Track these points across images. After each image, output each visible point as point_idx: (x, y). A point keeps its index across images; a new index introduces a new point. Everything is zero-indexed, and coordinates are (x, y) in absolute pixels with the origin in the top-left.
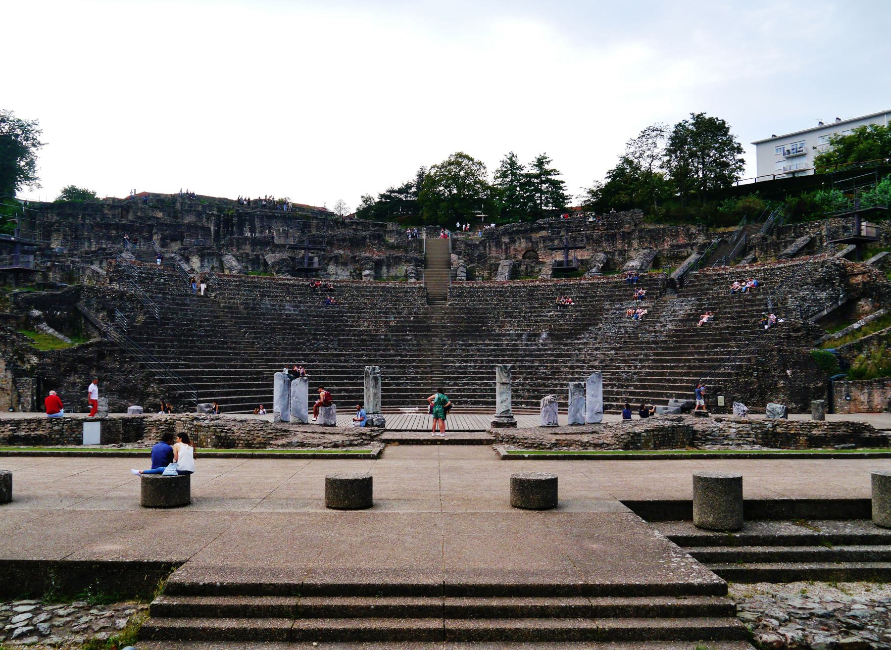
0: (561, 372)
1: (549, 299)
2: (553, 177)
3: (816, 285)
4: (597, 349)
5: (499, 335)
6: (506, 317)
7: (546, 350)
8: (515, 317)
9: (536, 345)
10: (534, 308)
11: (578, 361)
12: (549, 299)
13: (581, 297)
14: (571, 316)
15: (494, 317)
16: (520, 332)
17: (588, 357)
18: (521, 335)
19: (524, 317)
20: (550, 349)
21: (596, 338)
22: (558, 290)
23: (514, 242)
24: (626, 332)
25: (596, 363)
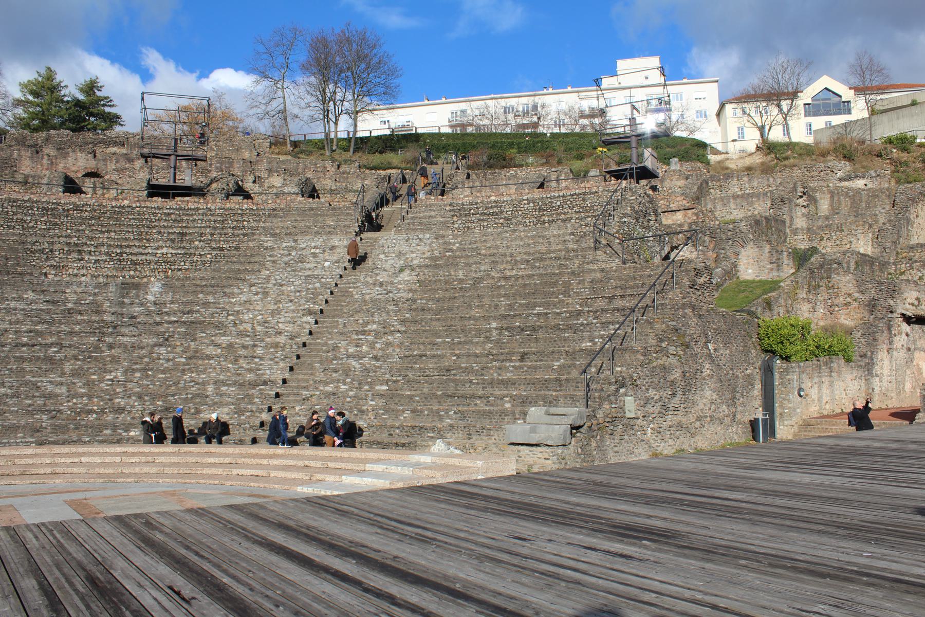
0: (209, 357)
1: (154, 227)
2: (107, 109)
3: (637, 219)
4: (273, 313)
5: (58, 283)
6: (69, 252)
7: (166, 313)
8: (90, 253)
9: (142, 304)
10: (126, 239)
11: (240, 334)
12: (154, 227)
13: (215, 228)
14: (205, 255)
15: (42, 251)
16: (101, 280)
17: (259, 328)
18: (106, 285)
19: (107, 254)
20: (175, 313)
21: (266, 294)
22: (169, 215)
23: (65, 156)
24: (323, 285)
25: (282, 339)
